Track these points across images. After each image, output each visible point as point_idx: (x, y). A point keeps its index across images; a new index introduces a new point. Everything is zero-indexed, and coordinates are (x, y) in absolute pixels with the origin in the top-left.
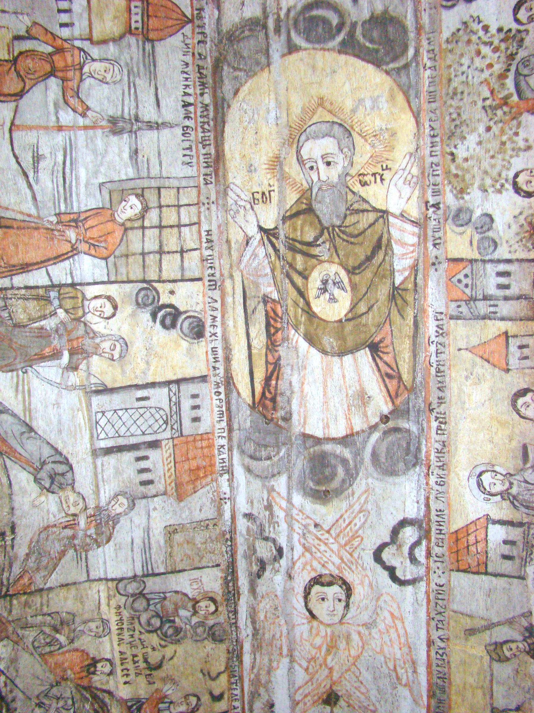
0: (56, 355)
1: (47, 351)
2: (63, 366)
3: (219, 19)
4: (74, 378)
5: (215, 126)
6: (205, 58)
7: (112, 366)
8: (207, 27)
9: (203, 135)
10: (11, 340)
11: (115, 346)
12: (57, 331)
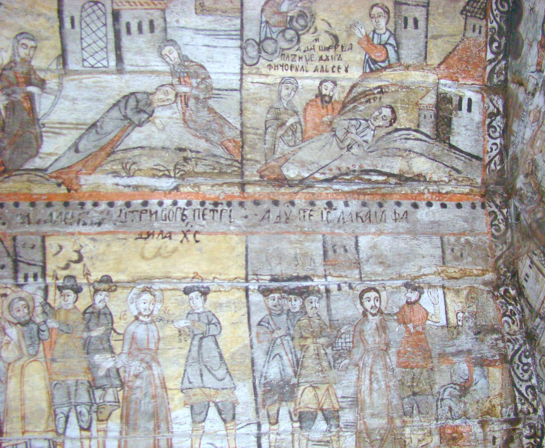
0: (30, 97)
1: (26, 105)
2: (40, 92)
4: (52, 83)
7: (41, 48)
10: (15, 135)
11: (23, 44)
12: (8, 95)
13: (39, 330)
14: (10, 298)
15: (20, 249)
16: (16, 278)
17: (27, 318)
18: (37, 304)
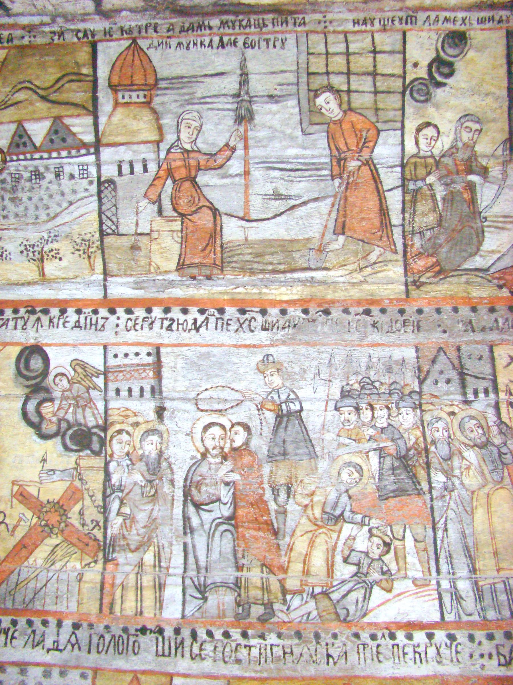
0: (471, 187)
1: (466, 196)
2: (482, 181)
3: (131, 10)
4: (495, 172)
5: (242, 13)
6: (172, 24)
7: (486, 132)
8: (140, 24)
9: (253, 27)
10: (453, 230)
11: (466, 127)
12: (447, 185)
13: (500, 453)
14: (459, 417)
15: (466, 361)
16: (464, 394)
17: (484, 439)
18: (491, 424)
